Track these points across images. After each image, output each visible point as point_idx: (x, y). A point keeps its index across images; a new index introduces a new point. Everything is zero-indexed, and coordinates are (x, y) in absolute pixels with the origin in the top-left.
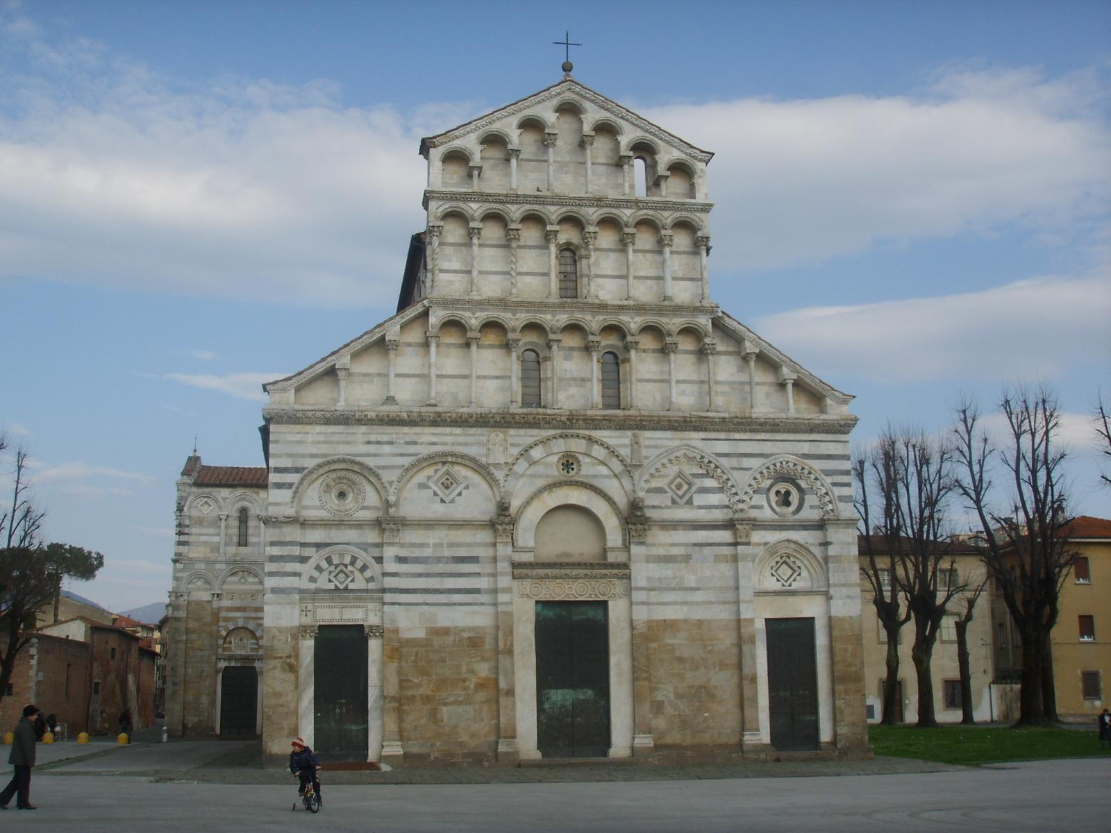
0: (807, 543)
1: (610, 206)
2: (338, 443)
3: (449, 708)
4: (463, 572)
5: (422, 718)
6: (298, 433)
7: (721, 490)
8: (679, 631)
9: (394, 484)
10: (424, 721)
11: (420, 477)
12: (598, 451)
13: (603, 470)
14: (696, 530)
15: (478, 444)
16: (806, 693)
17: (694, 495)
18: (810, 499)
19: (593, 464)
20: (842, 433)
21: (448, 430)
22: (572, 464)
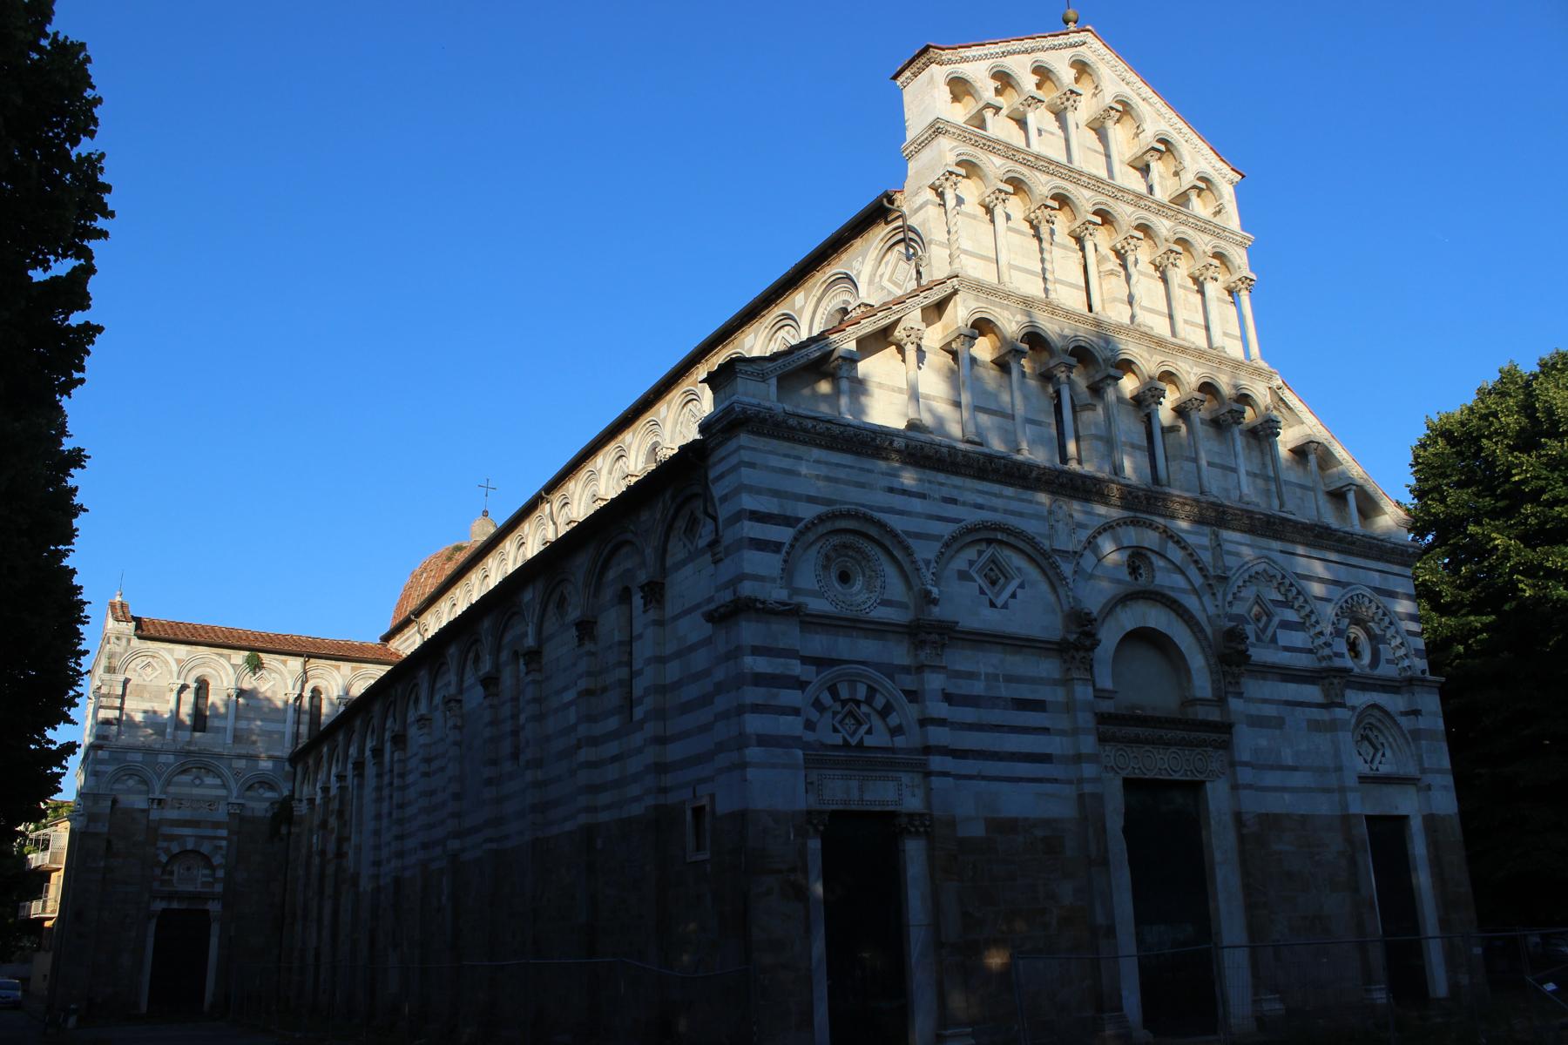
1: (1148, 209)
4: (1027, 724)
9: (932, 566)
11: (960, 562)
13: (1179, 581)
17: (1277, 630)
21: (996, 488)
22: (1139, 567)
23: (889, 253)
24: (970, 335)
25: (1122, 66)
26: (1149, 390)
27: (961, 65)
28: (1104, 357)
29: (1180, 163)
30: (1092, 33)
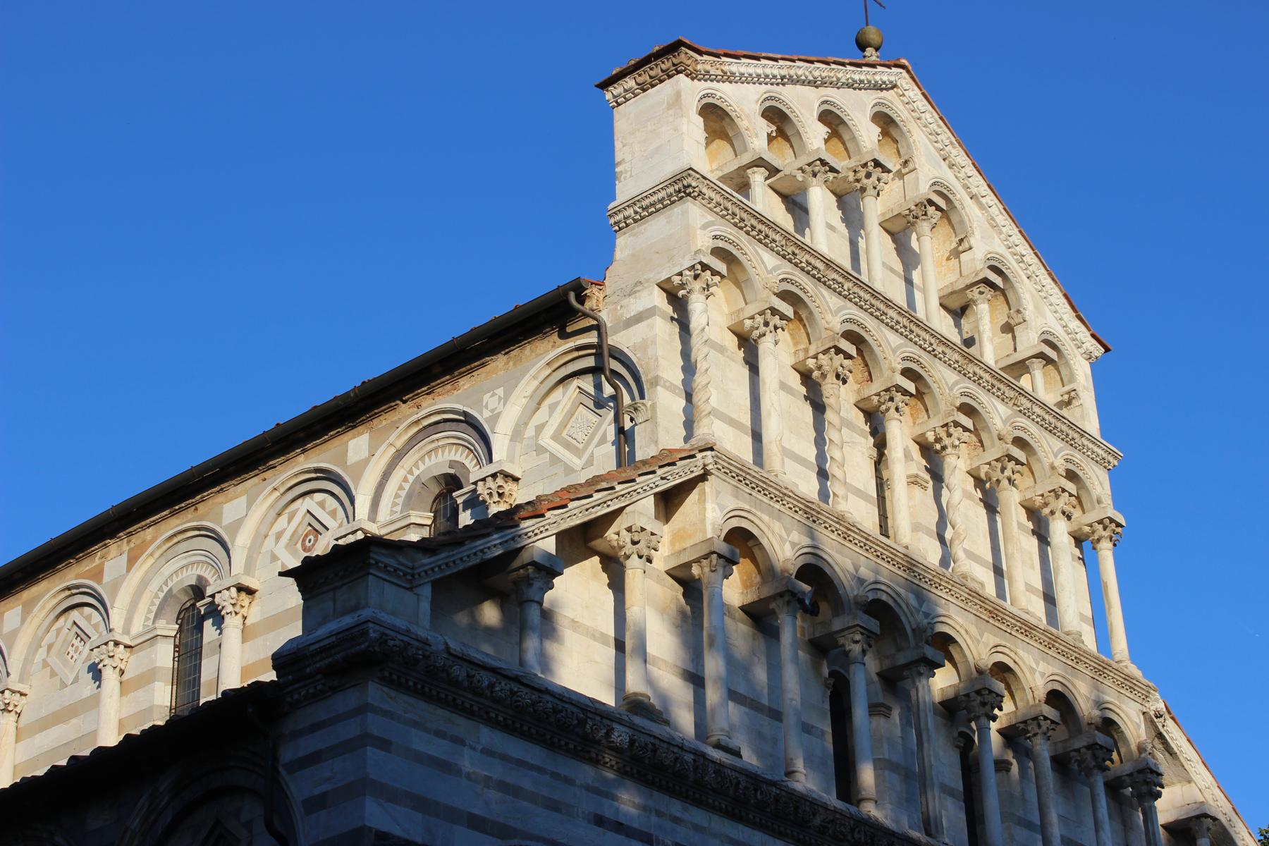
1: (977, 380)
23: (560, 390)
24: (727, 555)
25: (946, 136)
26: (978, 692)
28: (914, 627)
29: (1018, 311)
30: (908, 72)
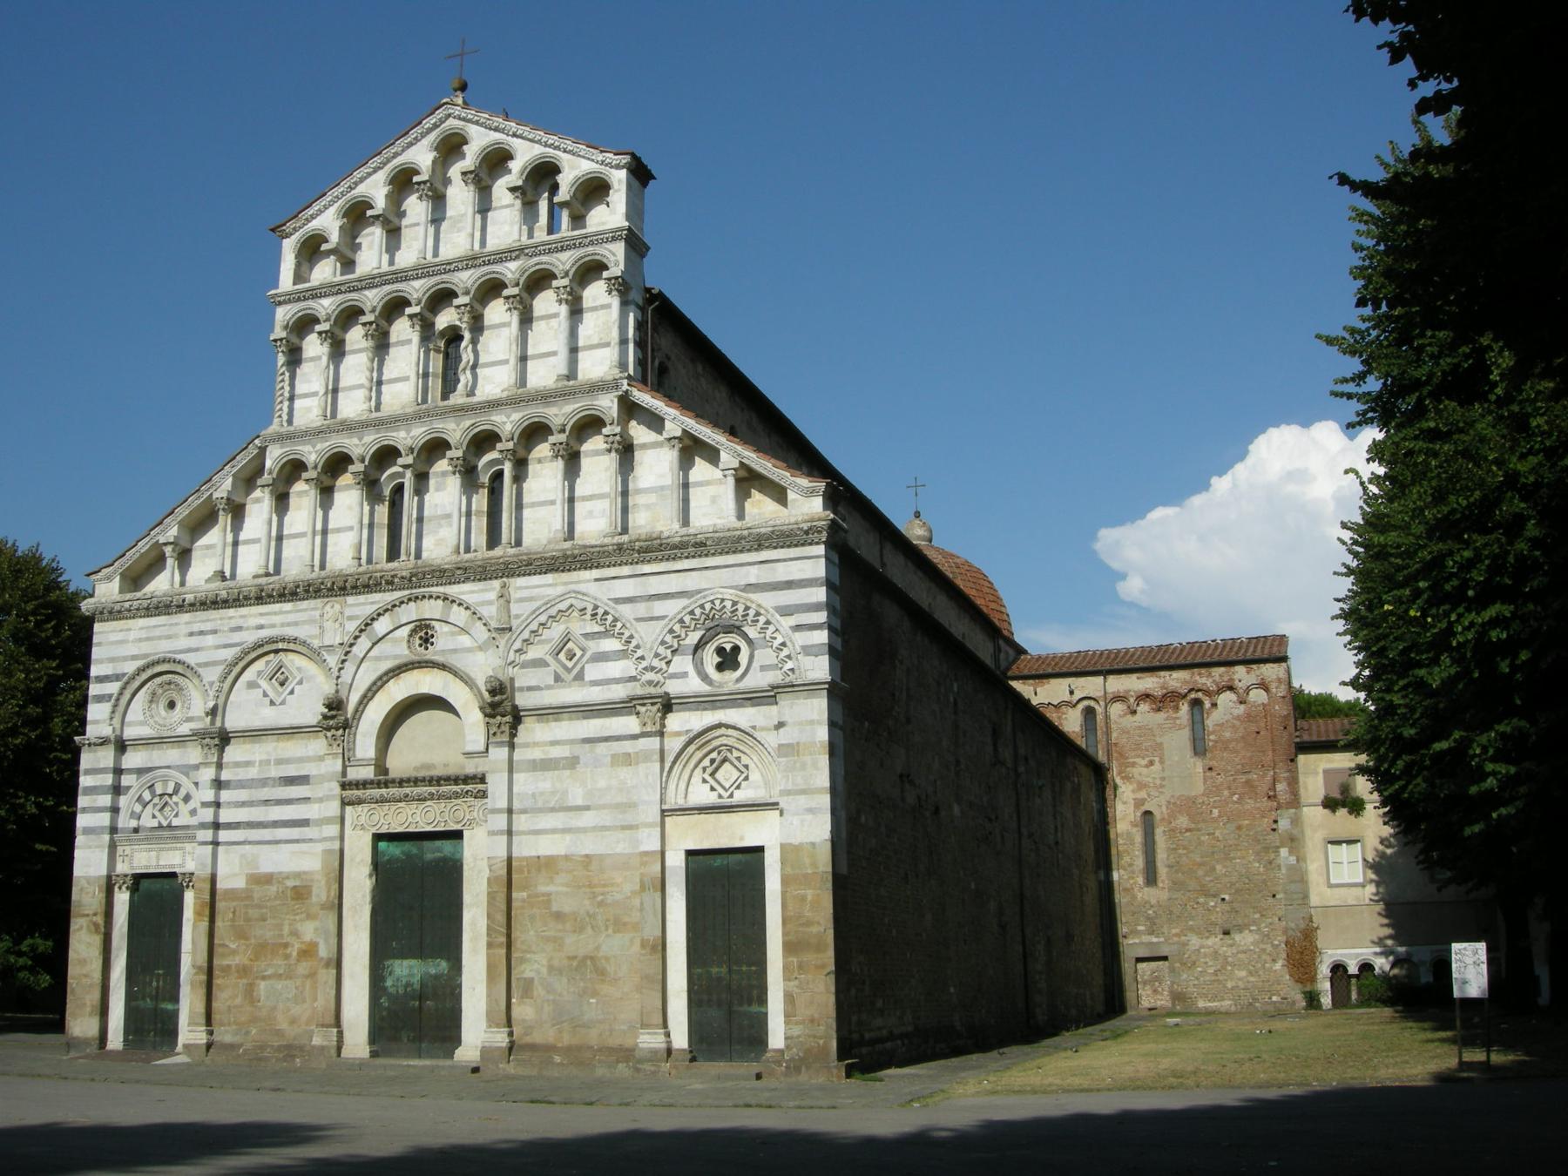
0: (754, 727)
2: (160, 638)
3: (268, 982)
5: (237, 996)
6: (121, 631)
7: (623, 654)
8: (558, 873)
10: (238, 1001)
11: (249, 674)
12: (458, 615)
13: (465, 641)
14: (585, 718)
15: (311, 621)
16: (753, 968)
18: (765, 656)
19: (453, 634)
20: (810, 544)
21: (277, 607)
22: (432, 636)
27: (310, 225)
